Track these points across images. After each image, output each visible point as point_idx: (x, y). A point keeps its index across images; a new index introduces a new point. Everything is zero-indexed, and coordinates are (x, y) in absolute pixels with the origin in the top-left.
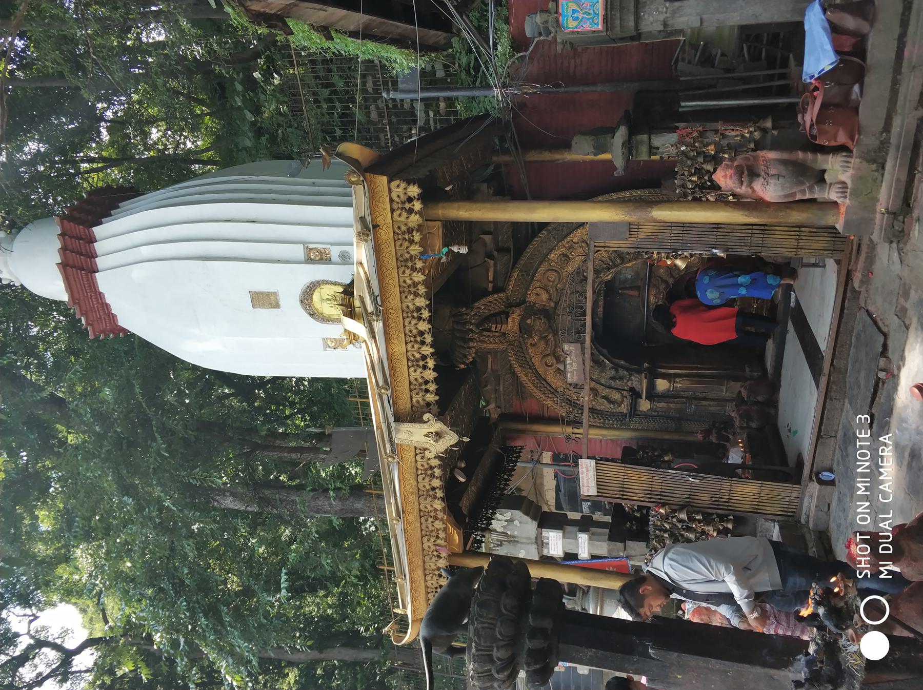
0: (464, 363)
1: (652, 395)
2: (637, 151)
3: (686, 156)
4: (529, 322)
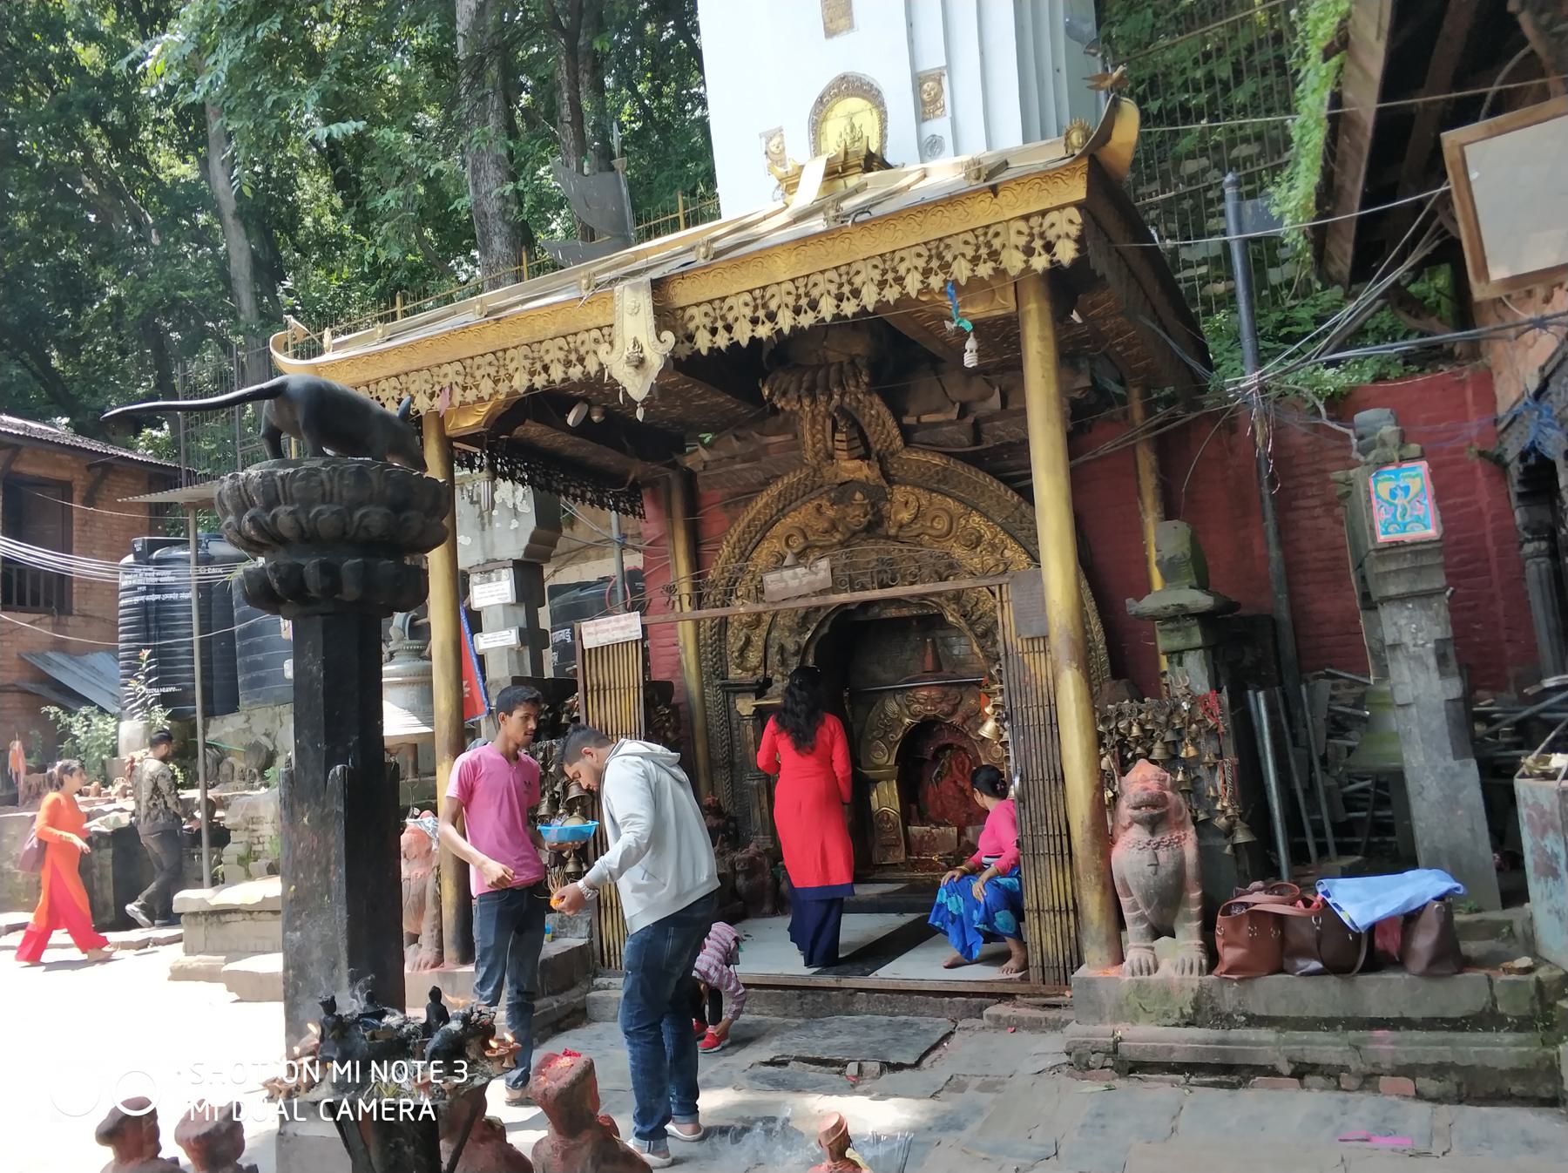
0: (772, 393)
2: (1172, 631)
3: (1171, 713)
4: (858, 496)
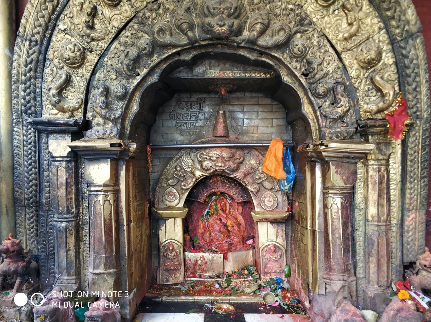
1: (77, 157)
